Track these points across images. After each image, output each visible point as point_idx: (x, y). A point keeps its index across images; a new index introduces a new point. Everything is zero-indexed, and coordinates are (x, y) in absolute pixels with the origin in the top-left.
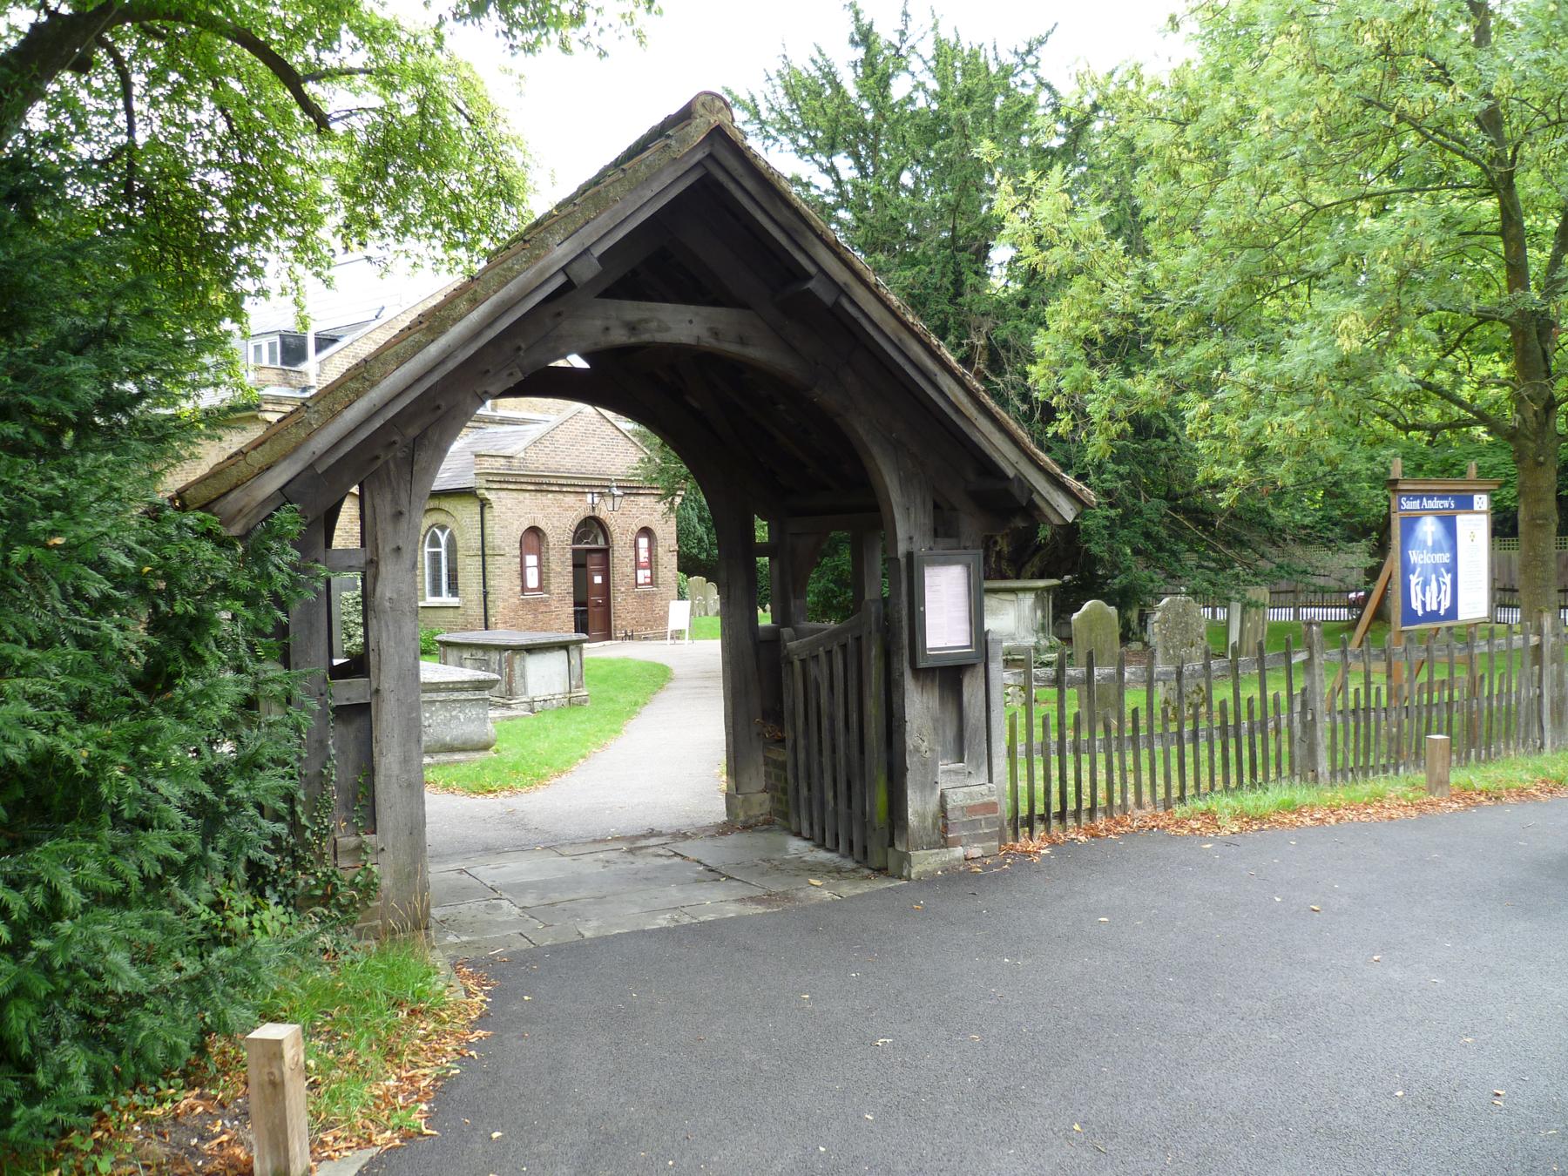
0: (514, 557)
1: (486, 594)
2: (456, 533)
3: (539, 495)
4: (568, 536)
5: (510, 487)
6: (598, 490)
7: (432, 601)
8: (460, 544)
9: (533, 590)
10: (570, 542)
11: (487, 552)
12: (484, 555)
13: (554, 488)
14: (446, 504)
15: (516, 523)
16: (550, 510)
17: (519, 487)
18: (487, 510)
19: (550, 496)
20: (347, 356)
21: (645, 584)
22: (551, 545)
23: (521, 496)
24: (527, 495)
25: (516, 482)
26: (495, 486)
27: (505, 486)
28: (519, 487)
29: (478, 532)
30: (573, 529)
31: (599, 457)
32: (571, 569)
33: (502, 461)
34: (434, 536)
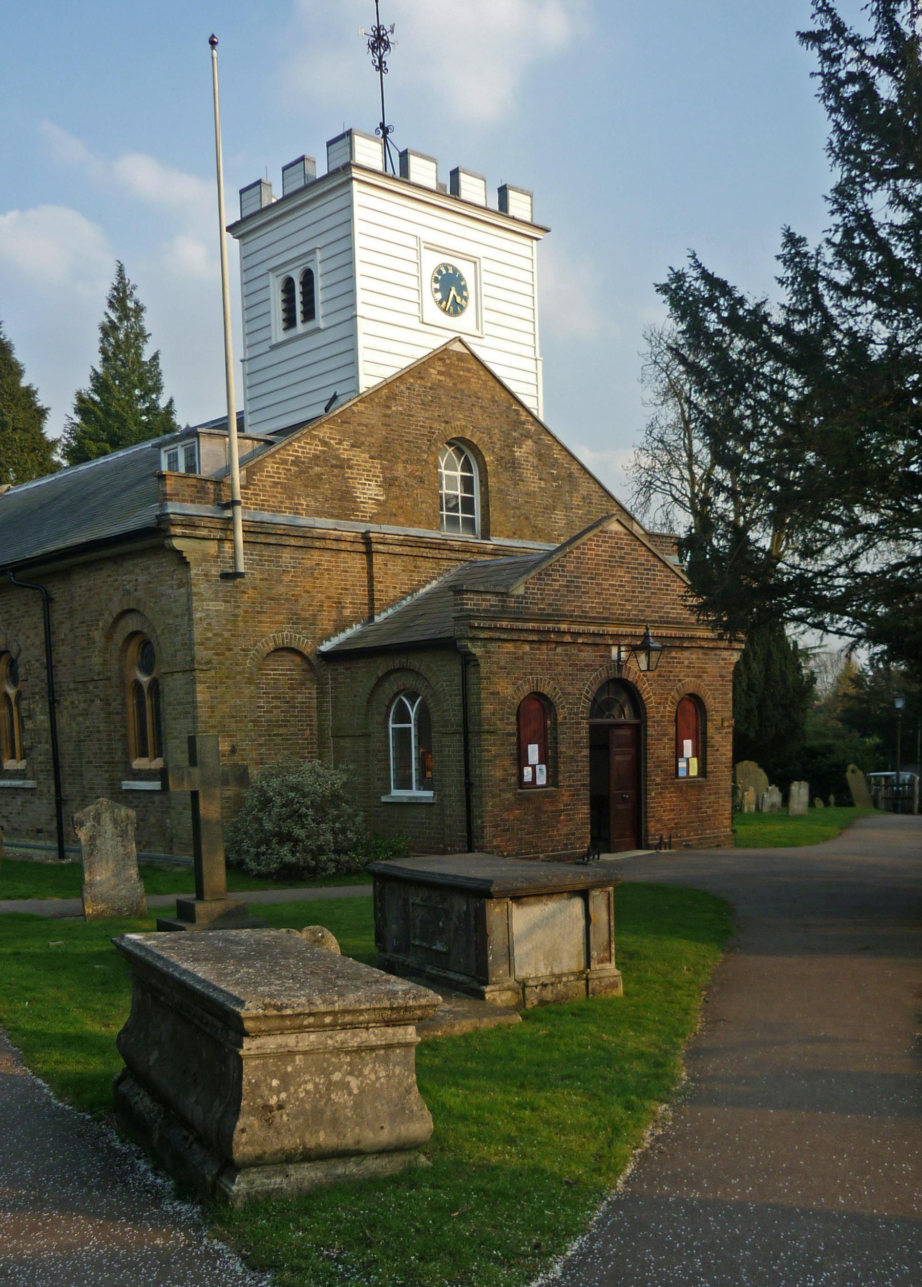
0: (509, 735)
1: (468, 786)
2: (431, 703)
4: (584, 706)
5: (504, 636)
6: (626, 642)
7: (397, 794)
8: (435, 718)
11: (471, 728)
12: (466, 733)
14: (416, 662)
18: (471, 670)
19: (559, 650)
20: (284, 462)
22: (560, 718)
26: (482, 635)
29: (458, 700)
32: (586, 752)
33: (493, 600)
34: (401, 705)
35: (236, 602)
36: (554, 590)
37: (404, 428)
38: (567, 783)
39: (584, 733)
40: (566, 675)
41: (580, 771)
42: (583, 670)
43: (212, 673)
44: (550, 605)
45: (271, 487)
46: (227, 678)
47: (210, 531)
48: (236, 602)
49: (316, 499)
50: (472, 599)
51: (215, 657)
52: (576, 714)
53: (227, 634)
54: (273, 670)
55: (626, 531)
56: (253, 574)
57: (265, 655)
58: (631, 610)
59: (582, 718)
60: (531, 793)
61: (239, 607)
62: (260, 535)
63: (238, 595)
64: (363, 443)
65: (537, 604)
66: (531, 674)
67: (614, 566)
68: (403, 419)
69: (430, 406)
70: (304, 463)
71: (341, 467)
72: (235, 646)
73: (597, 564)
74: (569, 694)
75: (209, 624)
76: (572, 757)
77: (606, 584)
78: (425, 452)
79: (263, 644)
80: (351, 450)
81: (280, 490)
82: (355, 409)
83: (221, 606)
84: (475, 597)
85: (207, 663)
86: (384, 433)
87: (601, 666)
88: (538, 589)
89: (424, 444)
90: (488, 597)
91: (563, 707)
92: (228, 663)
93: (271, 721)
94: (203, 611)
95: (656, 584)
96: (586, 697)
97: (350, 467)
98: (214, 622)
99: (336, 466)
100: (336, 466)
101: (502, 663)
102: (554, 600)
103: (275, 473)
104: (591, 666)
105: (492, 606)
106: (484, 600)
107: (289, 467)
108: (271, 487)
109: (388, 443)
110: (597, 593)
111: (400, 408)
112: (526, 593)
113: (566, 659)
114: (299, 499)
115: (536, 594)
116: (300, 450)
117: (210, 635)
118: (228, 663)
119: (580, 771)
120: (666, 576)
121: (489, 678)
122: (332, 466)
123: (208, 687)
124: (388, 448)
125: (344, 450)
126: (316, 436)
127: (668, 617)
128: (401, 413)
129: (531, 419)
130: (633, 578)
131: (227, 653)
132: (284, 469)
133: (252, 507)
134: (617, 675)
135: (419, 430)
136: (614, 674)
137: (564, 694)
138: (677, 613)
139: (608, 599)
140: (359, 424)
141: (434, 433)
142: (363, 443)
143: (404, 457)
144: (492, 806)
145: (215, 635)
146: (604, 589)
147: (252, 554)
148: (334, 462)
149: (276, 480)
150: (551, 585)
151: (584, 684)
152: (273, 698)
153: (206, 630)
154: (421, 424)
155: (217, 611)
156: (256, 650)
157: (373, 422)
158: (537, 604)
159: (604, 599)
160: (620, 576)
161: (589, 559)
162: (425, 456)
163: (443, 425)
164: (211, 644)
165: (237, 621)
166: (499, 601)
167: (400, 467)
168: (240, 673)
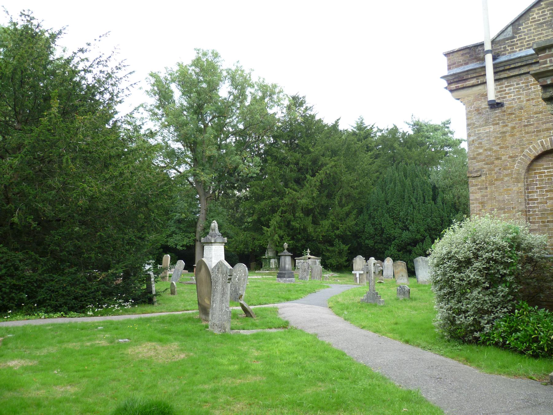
35: (504, 122)
43: (483, 178)
45: (535, 29)
46: (496, 180)
47: (478, 79)
48: (504, 122)
53: (495, 148)
54: (546, 169)
61: (507, 126)
62: (521, 68)
63: (506, 118)
72: (504, 155)
75: (481, 143)
79: (530, 150)
81: (545, 27)
83: (492, 128)
85: (477, 171)
93: (545, 210)
94: (475, 135)
98: (484, 142)
103: (540, 16)
117: (481, 151)
118: (497, 169)
123: (480, 189)
131: (496, 162)
132: (548, 11)
133: (518, 50)
145: (486, 150)
147: (517, 84)
149: (542, 21)
152: (547, 191)
153: (478, 148)
155: (486, 133)
156: (524, 155)
164: (482, 157)
168: (507, 175)
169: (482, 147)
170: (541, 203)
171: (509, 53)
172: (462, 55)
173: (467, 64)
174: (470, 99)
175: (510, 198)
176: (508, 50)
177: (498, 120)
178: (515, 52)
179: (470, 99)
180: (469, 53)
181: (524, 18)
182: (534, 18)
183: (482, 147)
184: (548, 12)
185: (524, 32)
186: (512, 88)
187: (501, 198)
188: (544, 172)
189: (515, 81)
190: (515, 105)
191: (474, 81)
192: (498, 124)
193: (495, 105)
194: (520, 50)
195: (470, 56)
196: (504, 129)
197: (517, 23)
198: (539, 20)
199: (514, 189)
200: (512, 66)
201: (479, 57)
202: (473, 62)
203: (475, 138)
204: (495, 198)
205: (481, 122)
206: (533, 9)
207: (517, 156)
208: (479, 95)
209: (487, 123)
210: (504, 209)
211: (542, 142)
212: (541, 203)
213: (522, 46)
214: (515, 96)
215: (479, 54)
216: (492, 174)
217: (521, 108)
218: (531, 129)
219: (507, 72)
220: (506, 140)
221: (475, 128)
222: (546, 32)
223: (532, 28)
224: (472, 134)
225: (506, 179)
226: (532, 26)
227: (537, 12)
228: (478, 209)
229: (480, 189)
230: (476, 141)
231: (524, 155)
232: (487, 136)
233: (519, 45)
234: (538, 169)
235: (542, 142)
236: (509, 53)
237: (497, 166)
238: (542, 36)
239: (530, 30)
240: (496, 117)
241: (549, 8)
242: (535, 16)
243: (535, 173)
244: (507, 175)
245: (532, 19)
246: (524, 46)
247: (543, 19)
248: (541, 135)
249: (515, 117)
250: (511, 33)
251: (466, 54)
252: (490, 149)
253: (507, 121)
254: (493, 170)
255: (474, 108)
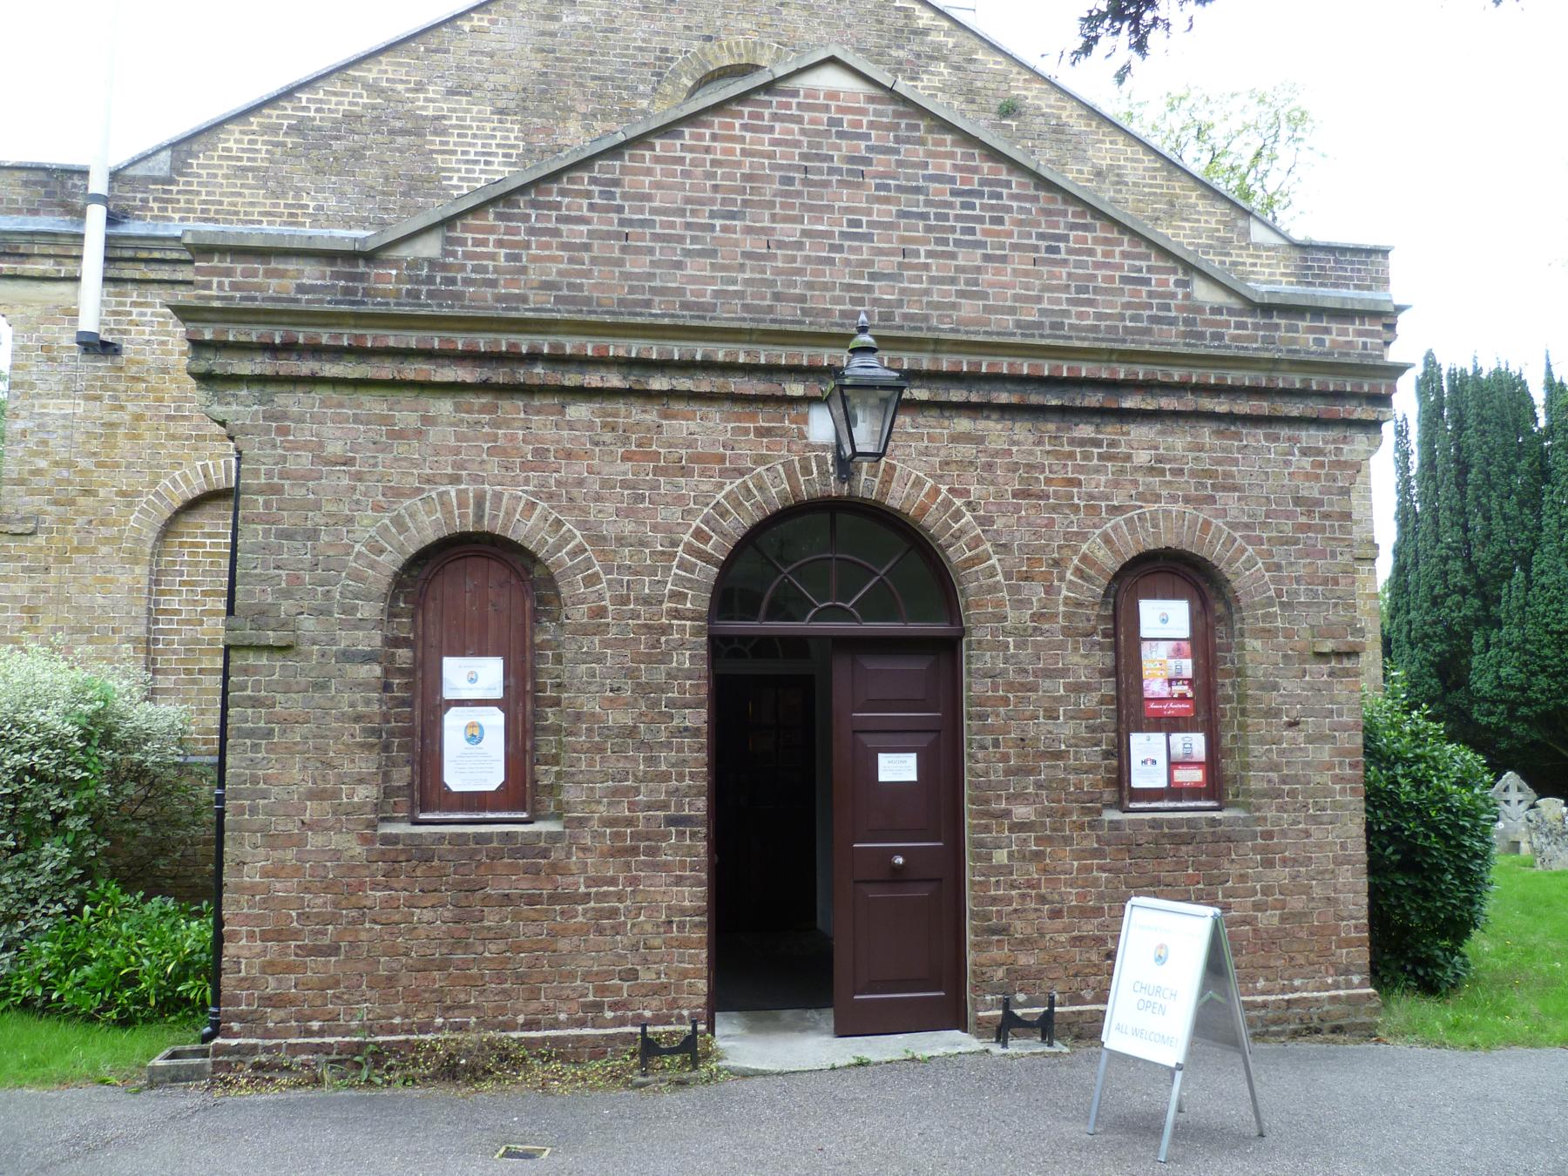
3: (512, 408)
9: (474, 801)
10: (697, 601)
13: (593, 379)
15: (367, 525)
16: (580, 468)
17: (385, 370)
19: (579, 411)
21: (1174, 792)
23: (406, 411)
24: (443, 406)
25: (359, 352)
27: (306, 367)
28: (385, 370)
30: (717, 547)
31: (884, 264)
35: (116, 398)
36: (565, 246)
37: (591, 53)
38: (602, 810)
39: (683, 660)
40: (605, 484)
41: (665, 777)
42: (685, 472)
43: (41, 540)
44: (547, 286)
45: (226, 177)
46: (77, 550)
47: (59, 264)
48: (116, 398)
49: (343, 194)
50: (228, 273)
51: (49, 508)
52: (647, 601)
53: (83, 463)
54: (210, 535)
55: (872, 91)
56: (163, 343)
57: (177, 504)
58: (900, 303)
59: (677, 614)
60: (441, 838)
61: (122, 408)
63: (121, 386)
64: (478, 87)
65: (493, 283)
66: (455, 480)
67: (826, 184)
68: (590, 38)
69: (664, 11)
70: (320, 129)
71: (418, 132)
72: (104, 485)
73: (748, 178)
74: (621, 540)
76: (632, 732)
77: (788, 231)
78: (643, 96)
79: (174, 482)
80: (445, 101)
81: (250, 181)
82: (466, 26)
83: (81, 407)
84: (239, 267)
85: (24, 520)
86: (537, 65)
87: (760, 460)
88: (500, 243)
89: (644, 81)
90: (292, 265)
91: (592, 580)
92: (81, 521)
93: (198, 641)
94: (32, 416)
95: (1010, 234)
96: (690, 549)
97: (443, 132)
98: (55, 442)
99: (404, 132)
100: (404, 132)
101: (334, 448)
102: (560, 273)
103: (244, 150)
104: (722, 459)
105: (301, 289)
106: (269, 274)
107: (281, 139)
108: (226, 177)
109: (548, 84)
110: (746, 255)
111: (584, 19)
112: (447, 253)
113: (608, 437)
114: (297, 196)
115: (493, 257)
116: (313, 107)
117: (42, 464)
118: (81, 521)
119: (665, 777)
120: (1048, 213)
121: (276, 490)
122: (392, 132)
123: (25, 569)
124: (544, 92)
125: (427, 100)
126: (355, 79)
127: (1057, 326)
128: (586, 27)
129: (946, 24)
130: (903, 215)
131: (81, 500)
132: (265, 143)
133: (177, 216)
134: (834, 488)
135: (634, 57)
136: (820, 483)
137: (597, 539)
138: (1099, 316)
139: (800, 272)
140: (472, 53)
141: (671, 60)
142: (478, 87)
143: (582, 108)
144: (265, 874)
145: (57, 464)
146: (781, 245)
148: (398, 124)
149: (245, 163)
150: (556, 233)
151: (687, 513)
152: (205, 594)
154: (640, 43)
155: (65, 417)
156: (157, 494)
157: (509, 46)
158: (493, 283)
159: (778, 271)
160: (848, 210)
161: (714, 163)
162: (644, 103)
163: (697, 44)
164: (45, 483)
165: (115, 435)
166: (336, 276)
167: (574, 126)
168: (107, 541)
169: (47, 454)
170: (188, 622)
171: (154, 218)
172: (26, 184)
173: (34, 212)
174: (29, 312)
175: (108, 602)
176: (152, 209)
177: (101, 388)
178: (169, 219)
179: (29, 312)
180: (44, 184)
181: (203, 139)
182: (229, 150)
183: (47, 454)
184: (264, 148)
185: (199, 176)
186: (149, 311)
187: (84, 601)
188: (204, 545)
189: (159, 296)
190: (150, 358)
191: (46, 267)
192: (98, 398)
193: (97, 347)
194: (182, 219)
195: (48, 194)
196: (115, 417)
197: (185, 147)
198: (240, 159)
199: (123, 579)
200: (156, 255)
201: (73, 205)
202: (52, 213)
203: (31, 424)
204: (68, 599)
205: (54, 382)
206: (229, 127)
207: (140, 494)
208: (57, 307)
209: (68, 390)
210: (89, 630)
211: (205, 468)
212: (188, 622)
213: (189, 210)
214: (152, 333)
215: (75, 195)
216: (65, 532)
217: (165, 371)
218: (183, 428)
219: (142, 266)
220: (114, 447)
221: (33, 397)
222: (252, 195)
223: (220, 172)
224: (23, 413)
225: (104, 550)
226: (221, 166)
227: (237, 136)
228: (18, 625)
229: (25, 569)
230: (33, 432)
231: (157, 494)
232: (64, 427)
233: (182, 205)
234: (189, 535)
235: (205, 468)
236: (154, 218)
237: (84, 513)
238: (240, 200)
239: (215, 176)
240: (97, 378)
241: (266, 138)
242: (231, 144)
243: (181, 545)
244: (107, 541)
245: (224, 149)
246: (193, 211)
247: (249, 159)
248: (204, 448)
249: (147, 390)
250: (166, 168)
251: (35, 183)
252: (70, 465)
253: (123, 396)
254: (71, 522)
255: (38, 340)
